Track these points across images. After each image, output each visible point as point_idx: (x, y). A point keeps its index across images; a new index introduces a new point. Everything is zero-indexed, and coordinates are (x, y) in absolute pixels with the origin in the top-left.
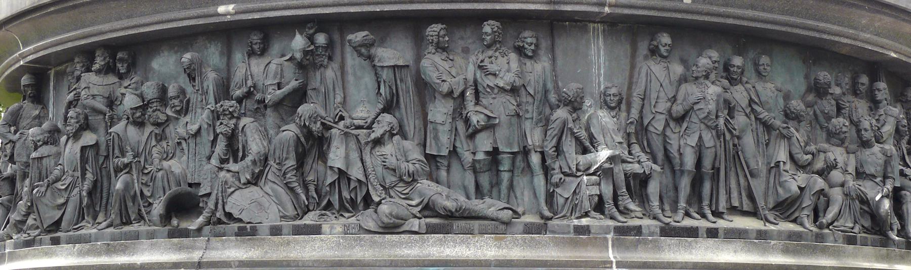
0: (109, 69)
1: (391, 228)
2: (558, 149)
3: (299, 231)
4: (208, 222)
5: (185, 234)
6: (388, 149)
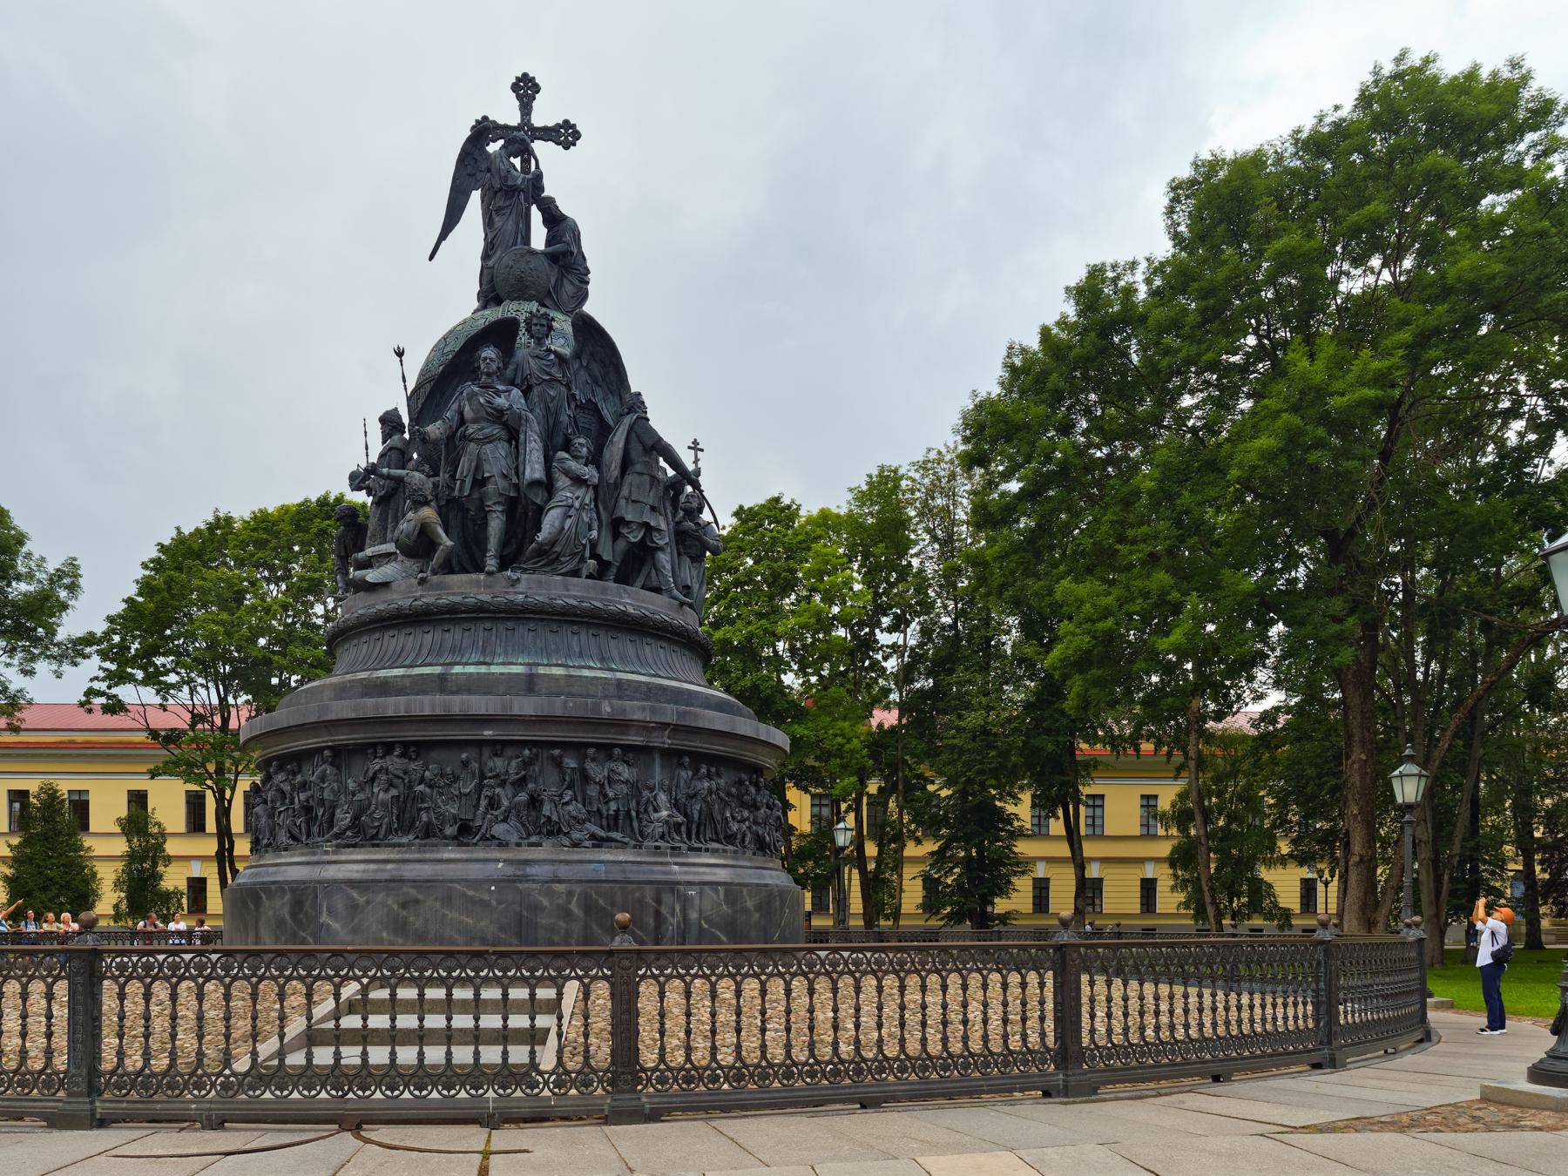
0: (402, 755)
2: (646, 811)
3: (531, 845)
4: (481, 839)
5: (467, 845)
6: (571, 808)
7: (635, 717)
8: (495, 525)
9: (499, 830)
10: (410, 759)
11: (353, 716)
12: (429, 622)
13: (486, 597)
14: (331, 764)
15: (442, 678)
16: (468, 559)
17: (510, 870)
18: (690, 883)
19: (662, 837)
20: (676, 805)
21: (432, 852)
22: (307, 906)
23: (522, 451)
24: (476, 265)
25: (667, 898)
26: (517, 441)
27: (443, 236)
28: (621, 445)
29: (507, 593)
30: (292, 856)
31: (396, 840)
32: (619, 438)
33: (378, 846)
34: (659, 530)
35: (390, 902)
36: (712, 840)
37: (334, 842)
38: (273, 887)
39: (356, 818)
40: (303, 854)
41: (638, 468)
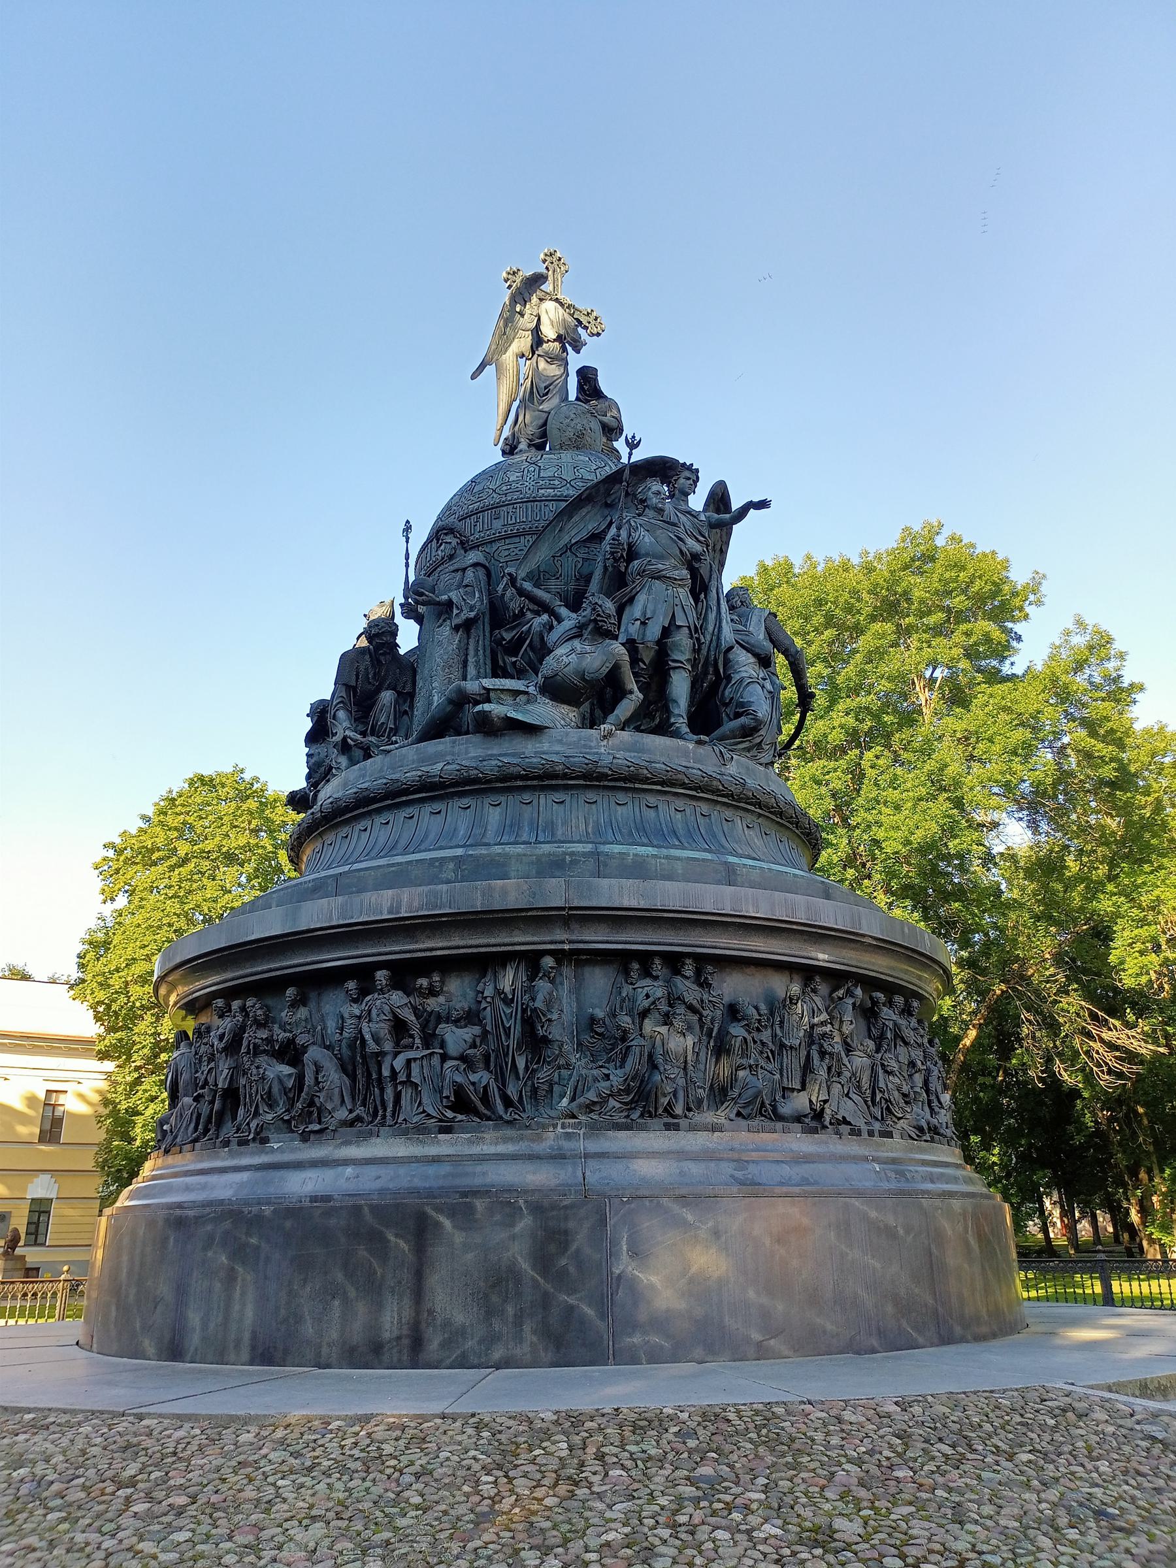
11: (643, 904)
22: (581, 1240)
33: (677, 1127)
40: (506, 1140)
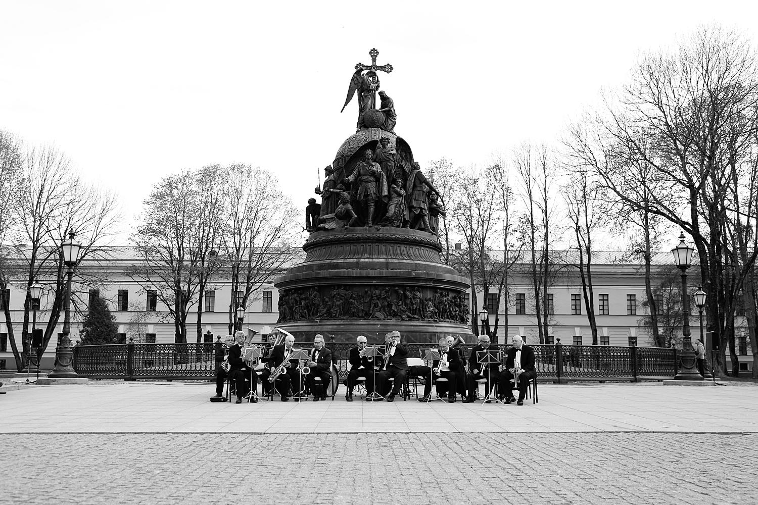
1: (403, 319)
6: (401, 307)
7: (423, 277)
8: (372, 209)
9: (378, 314)
10: (347, 290)
11: (328, 276)
12: (349, 243)
13: (369, 235)
14: (318, 292)
15: (358, 263)
16: (362, 222)
17: (383, 328)
18: (441, 333)
19: (431, 317)
20: (435, 306)
21: (355, 321)
23: (381, 185)
24: (358, 114)
25: (433, 337)
26: (379, 181)
27: (346, 104)
28: (413, 181)
29: (376, 233)
30: (303, 323)
31: (342, 317)
32: (412, 179)
33: (336, 319)
34: (425, 209)
35: (342, 338)
36: (446, 318)
37: (320, 318)
38: (298, 333)
39: (329, 310)
41: (419, 189)
